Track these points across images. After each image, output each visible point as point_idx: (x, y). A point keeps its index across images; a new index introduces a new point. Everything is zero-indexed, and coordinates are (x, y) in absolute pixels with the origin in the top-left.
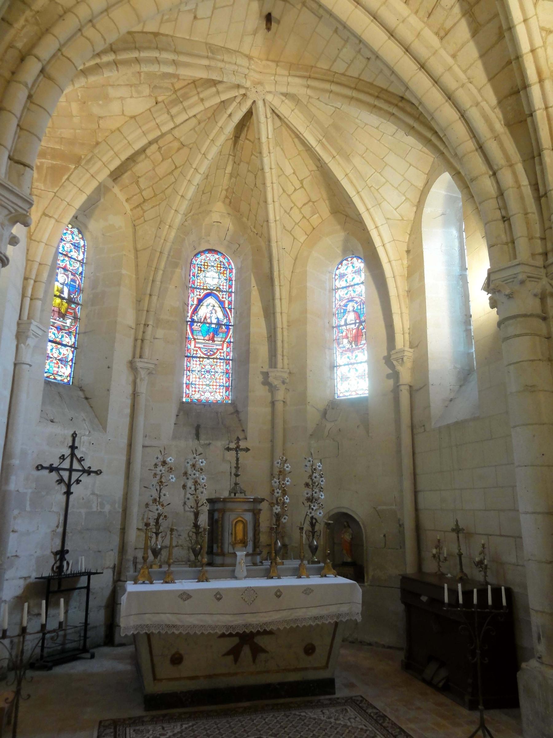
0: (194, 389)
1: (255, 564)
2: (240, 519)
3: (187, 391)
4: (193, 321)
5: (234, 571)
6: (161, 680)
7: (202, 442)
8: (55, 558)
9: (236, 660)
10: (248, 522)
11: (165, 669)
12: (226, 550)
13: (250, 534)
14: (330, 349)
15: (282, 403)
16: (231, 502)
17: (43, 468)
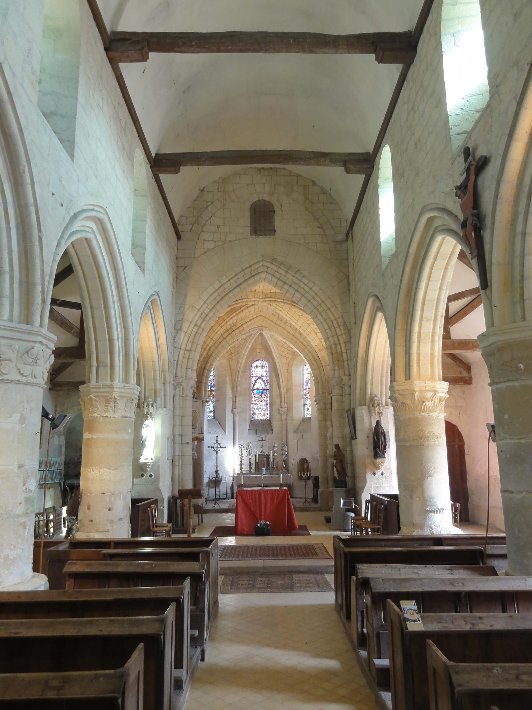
4: (253, 390)
14: (303, 398)
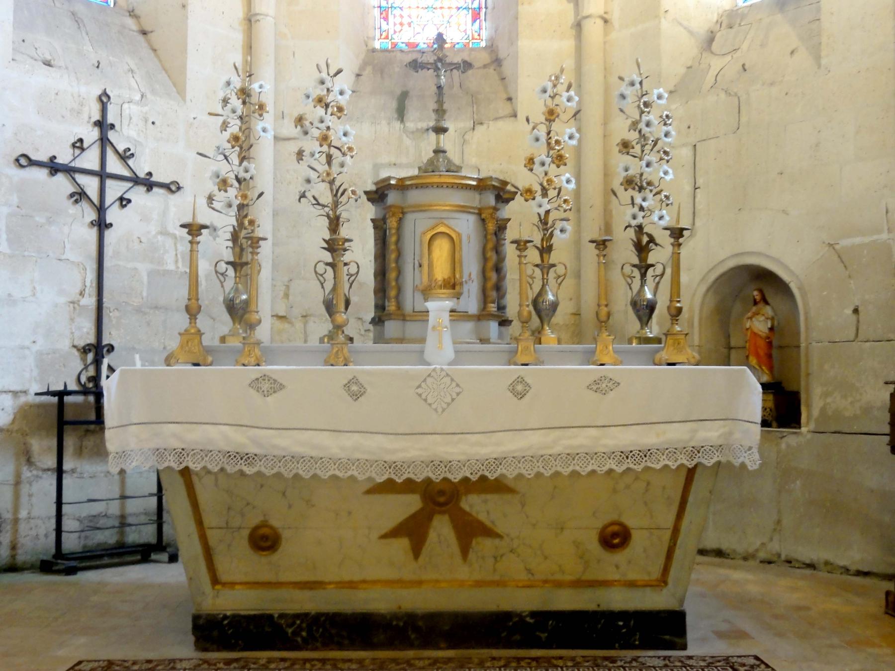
0: (398, 20)
1: (484, 341)
2: (442, 229)
3: (384, 23)
5: (422, 352)
6: (232, 584)
7: (410, 125)
8: (84, 360)
9: (416, 551)
10: (464, 238)
11: (238, 562)
12: (408, 307)
13: (471, 267)
15: (600, 22)
16: (417, 186)
17: (32, 163)
